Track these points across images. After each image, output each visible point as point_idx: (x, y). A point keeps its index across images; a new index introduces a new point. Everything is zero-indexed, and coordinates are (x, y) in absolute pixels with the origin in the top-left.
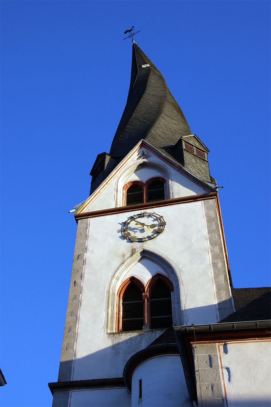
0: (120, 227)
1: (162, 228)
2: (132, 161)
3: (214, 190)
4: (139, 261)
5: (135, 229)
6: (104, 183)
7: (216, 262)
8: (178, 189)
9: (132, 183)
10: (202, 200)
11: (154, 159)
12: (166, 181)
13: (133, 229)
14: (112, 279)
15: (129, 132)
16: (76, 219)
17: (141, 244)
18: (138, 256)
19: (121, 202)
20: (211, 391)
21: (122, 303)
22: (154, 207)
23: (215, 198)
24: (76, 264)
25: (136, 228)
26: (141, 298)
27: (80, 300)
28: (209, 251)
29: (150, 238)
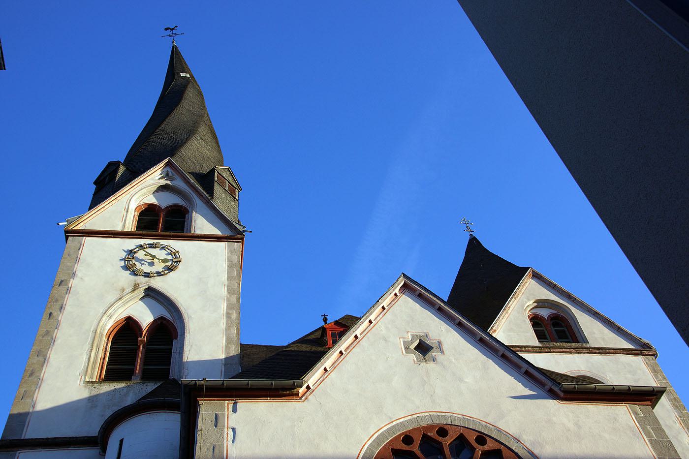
0: (124, 255)
1: (176, 265)
2: (152, 179)
3: (241, 233)
4: (141, 299)
5: (142, 260)
6: (112, 198)
7: (231, 312)
8: (201, 224)
9: (148, 206)
10: (226, 241)
11: (179, 183)
12: (189, 212)
13: (140, 260)
14: (103, 316)
15: (153, 145)
16: (66, 235)
17: (147, 279)
18: (141, 293)
19: (130, 225)
20: (212, 453)
21: (110, 347)
22: (170, 239)
23: (241, 242)
24: (56, 292)
25: (144, 259)
26: (136, 342)
27: (54, 338)
28: (224, 299)
29: (159, 274)
